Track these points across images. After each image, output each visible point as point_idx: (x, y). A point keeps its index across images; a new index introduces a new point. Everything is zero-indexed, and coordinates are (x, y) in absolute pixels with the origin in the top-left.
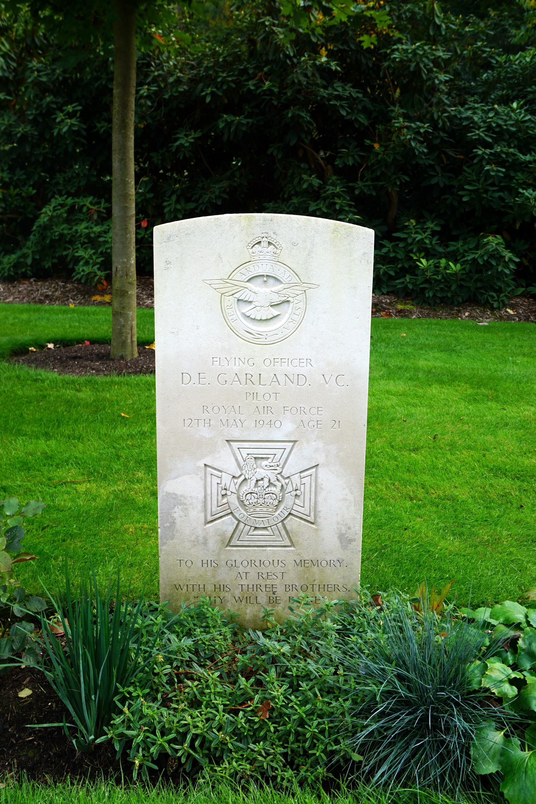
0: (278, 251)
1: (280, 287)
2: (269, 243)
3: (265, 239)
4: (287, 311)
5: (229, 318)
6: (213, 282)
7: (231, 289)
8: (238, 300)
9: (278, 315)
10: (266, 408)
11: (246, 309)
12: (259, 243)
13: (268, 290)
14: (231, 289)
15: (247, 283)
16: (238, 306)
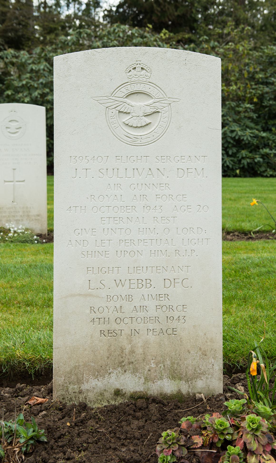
0: (149, 74)
1: (151, 101)
2: (142, 68)
3: (138, 65)
4: (156, 120)
5: (113, 126)
6: (101, 98)
7: (114, 103)
8: (119, 112)
9: (150, 123)
10: (142, 196)
11: (126, 118)
12: (135, 68)
13: (142, 104)
14: (114, 103)
15: (125, 99)
16: (119, 115)
